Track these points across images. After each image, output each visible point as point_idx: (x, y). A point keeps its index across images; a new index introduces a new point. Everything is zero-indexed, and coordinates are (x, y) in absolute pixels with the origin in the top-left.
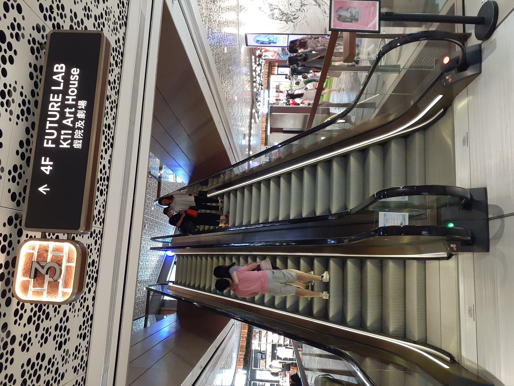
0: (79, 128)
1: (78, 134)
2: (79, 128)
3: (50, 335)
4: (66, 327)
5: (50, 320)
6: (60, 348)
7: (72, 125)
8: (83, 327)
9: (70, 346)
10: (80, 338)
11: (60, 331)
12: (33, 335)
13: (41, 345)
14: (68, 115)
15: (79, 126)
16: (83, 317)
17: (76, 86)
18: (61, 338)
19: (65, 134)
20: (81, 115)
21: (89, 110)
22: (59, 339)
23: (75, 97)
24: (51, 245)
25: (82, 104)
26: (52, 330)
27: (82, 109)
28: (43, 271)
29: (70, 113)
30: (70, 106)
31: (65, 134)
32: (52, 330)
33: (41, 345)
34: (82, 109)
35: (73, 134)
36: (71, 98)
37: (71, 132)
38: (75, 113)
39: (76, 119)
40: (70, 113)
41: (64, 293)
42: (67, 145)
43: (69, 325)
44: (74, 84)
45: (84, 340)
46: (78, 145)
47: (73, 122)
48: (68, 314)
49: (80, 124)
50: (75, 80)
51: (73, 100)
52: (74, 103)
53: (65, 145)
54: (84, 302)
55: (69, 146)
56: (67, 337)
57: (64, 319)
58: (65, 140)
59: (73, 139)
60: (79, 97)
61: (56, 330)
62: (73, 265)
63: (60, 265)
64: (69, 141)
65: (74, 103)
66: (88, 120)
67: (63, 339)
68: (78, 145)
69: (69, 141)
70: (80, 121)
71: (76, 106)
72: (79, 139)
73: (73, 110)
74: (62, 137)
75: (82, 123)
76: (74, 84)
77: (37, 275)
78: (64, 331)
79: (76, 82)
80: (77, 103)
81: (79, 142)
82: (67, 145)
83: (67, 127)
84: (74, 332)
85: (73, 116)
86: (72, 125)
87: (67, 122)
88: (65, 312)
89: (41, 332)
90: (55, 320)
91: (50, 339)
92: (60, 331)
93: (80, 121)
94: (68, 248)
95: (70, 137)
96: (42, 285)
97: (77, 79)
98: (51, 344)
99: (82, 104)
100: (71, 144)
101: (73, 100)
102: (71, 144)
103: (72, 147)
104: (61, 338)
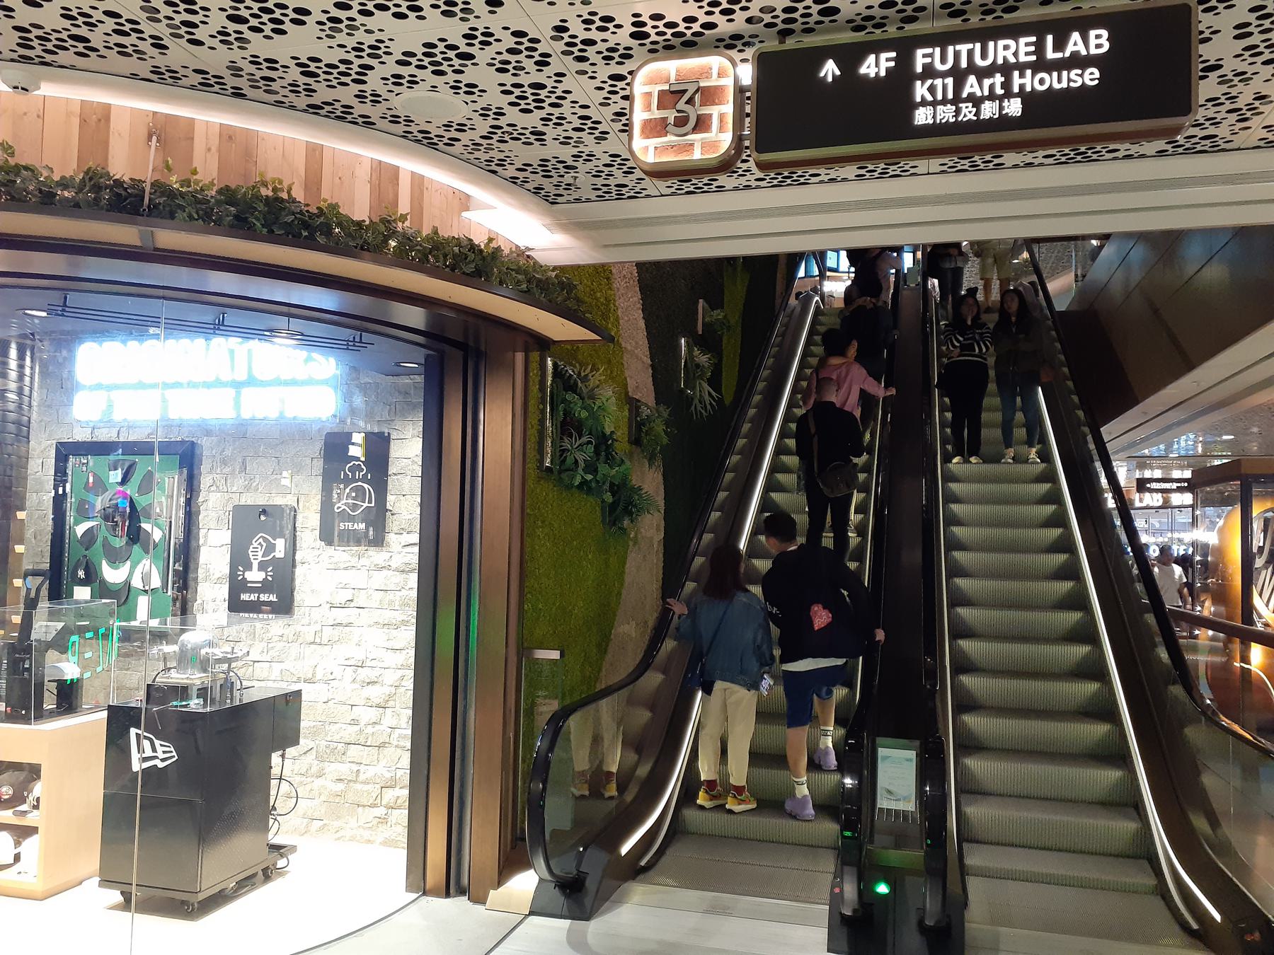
0: (958, 112)
1: (946, 114)
2: (958, 112)
7: (965, 95)
14: (987, 82)
15: (964, 111)
17: (1056, 86)
19: (945, 87)
20: (989, 110)
21: (1003, 122)
23: (1028, 89)
24: (728, 108)
25: (1014, 107)
27: (1001, 108)
28: (681, 105)
29: (992, 87)
30: (1007, 85)
31: (945, 87)
34: (1001, 108)
35: (944, 102)
36: (1027, 81)
37: (950, 96)
38: (992, 96)
39: (976, 101)
40: (992, 87)
41: (647, 150)
42: (923, 97)
44: (1059, 81)
46: (922, 116)
47: (972, 98)
49: (968, 112)
50: (1069, 80)
51: (1022, 87)
52: (1016, 90)
53: (921, 90)
55: (918, 99)
58: (932, 90)
59: (934, 104)
60: (1029, 98)
62: (697, 155)
63: (696, 129)
64: (929, 98)
65: (1016, 90)
66: (979, 126)
68: (922, 116)
69: (929, 98)
70: (974, 110)
71: (1008, 94)
72: (934, 117)
73: (999, 91)
74: (938, 82)
75: (971, 117)
76: (1059, 81)
77: (671, 96)
79: (1064, 85)
80: (1017, 95)
81: (930, 117)
82: (923, 97)
83: (958, 86)
85: (986, 93)
86: (965, 95)
87: (971, 85)
93: (974, 110)
94: (720, 139)
95: (940, 97)
96: (660, 106)
97: (1072, 84)
99: (1014, 107)
100: (924, 103)
101: (1022, 87)
102: (924, 103)
103: (916, 106)
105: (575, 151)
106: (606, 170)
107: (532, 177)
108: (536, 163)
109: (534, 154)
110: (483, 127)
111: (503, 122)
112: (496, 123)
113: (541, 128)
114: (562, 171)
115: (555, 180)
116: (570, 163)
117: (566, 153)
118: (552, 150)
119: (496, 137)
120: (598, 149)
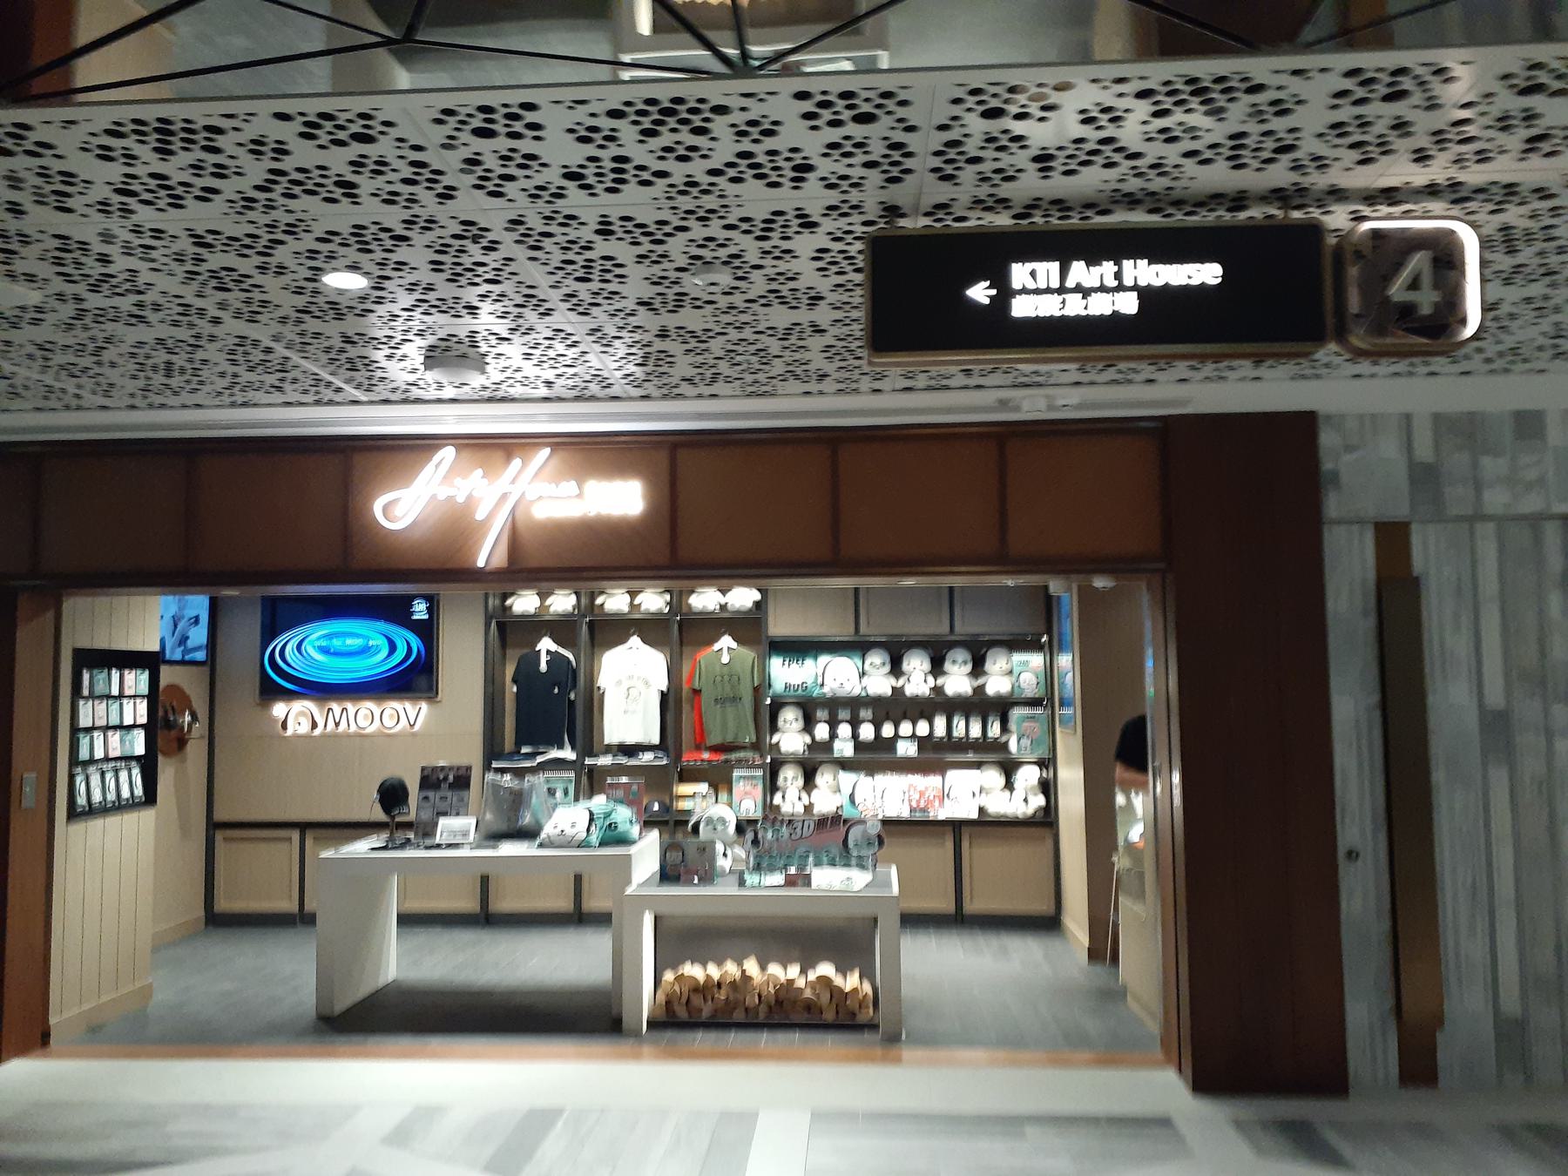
3: (601, 147)
4: (623, 181)
5: (641, 141)
6: (569, 176)
8: (629, 225)
9: (575, 199)
10: (601, 223)
11: (614, 170)
12: (666, 265)
13: (571, 131)
16: (658, 223)
18: (597, 175)
22: (591, 170)
26: (614, 150)
32: (614, 150)
33: (571, 131)
43: (631, 190)
45: (598, 232)
48: (661, 183)
54: (699, 219)
56: (599, 189)
57: (646, 176)
61: (616, 159)
67: (591, 180)
78: (614, 180)
84: (613, 206)
88: (662, 174)
89: (606, 123)
90: (639, 153)
91: (590, 150)
92: (614, 170)
98: (576, 154)
104: (597, 175)
105: (406, 215)
106: (456, 243)
107: (342, 251)
108: (346, 230)
109: (342, 217)
110: (257, 171)
111: (287, 164)
112: (276, 165)
113: (350, 178)
114: (388, 243)
115: (379, 255)
116: (400, 231)
117: (393, 217)
118: (370, 211)
119: (279, 189)
120: (442, 212)
